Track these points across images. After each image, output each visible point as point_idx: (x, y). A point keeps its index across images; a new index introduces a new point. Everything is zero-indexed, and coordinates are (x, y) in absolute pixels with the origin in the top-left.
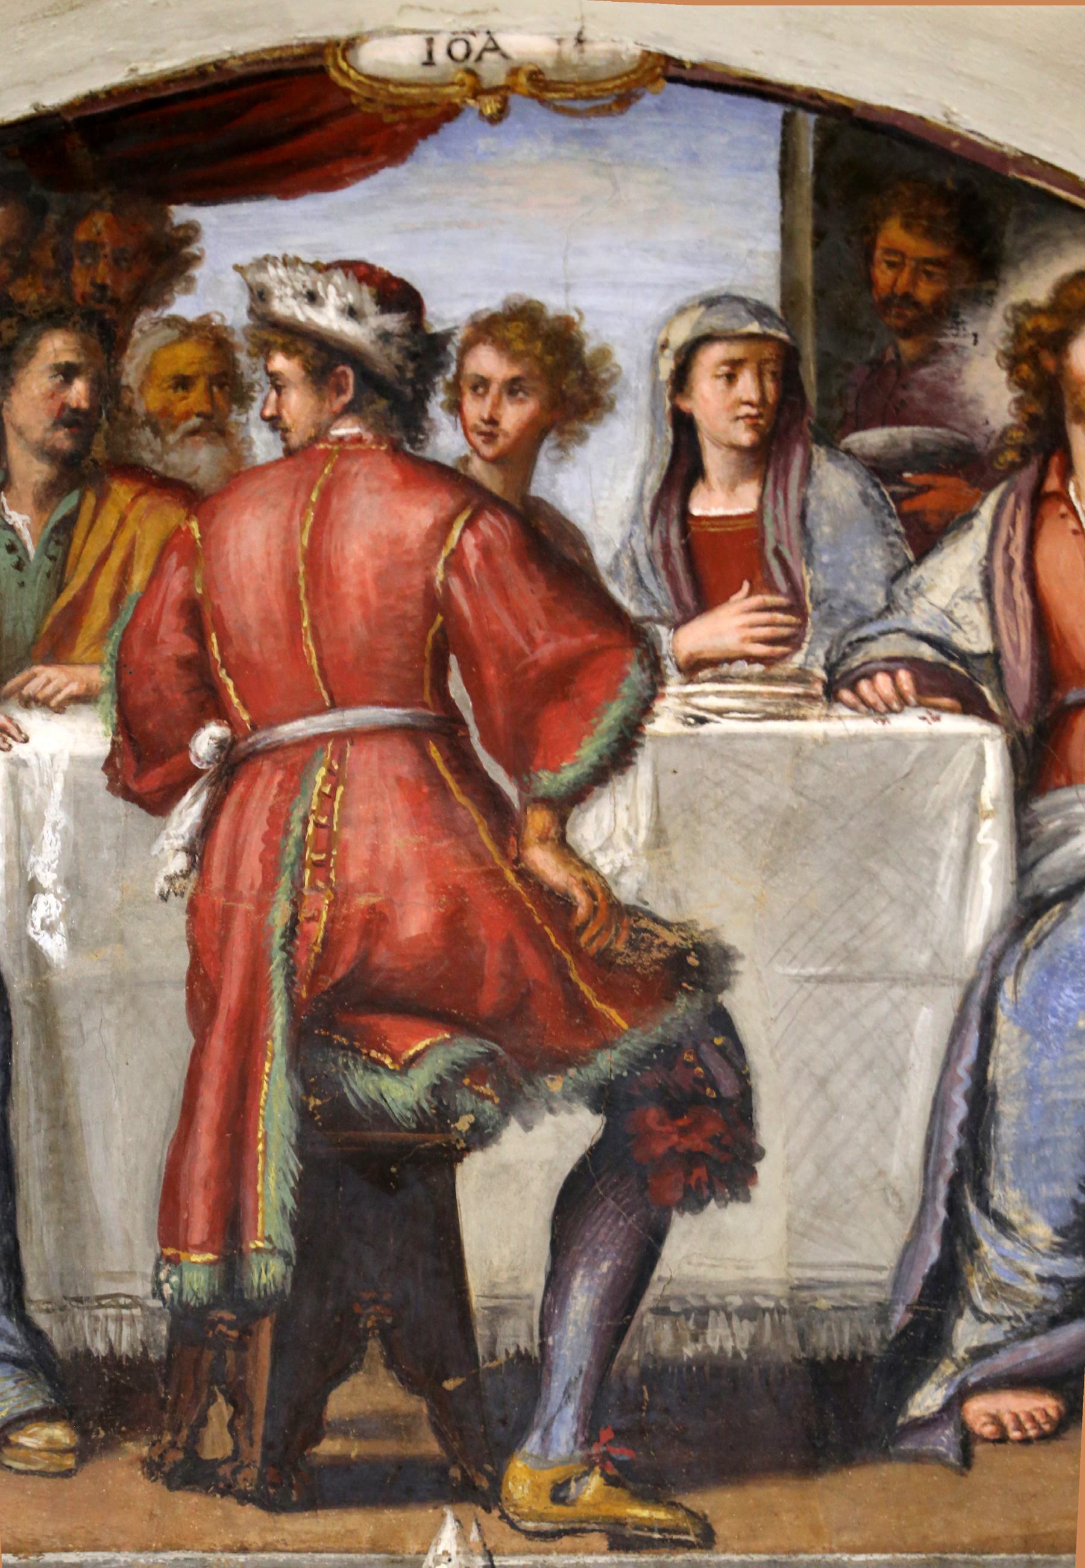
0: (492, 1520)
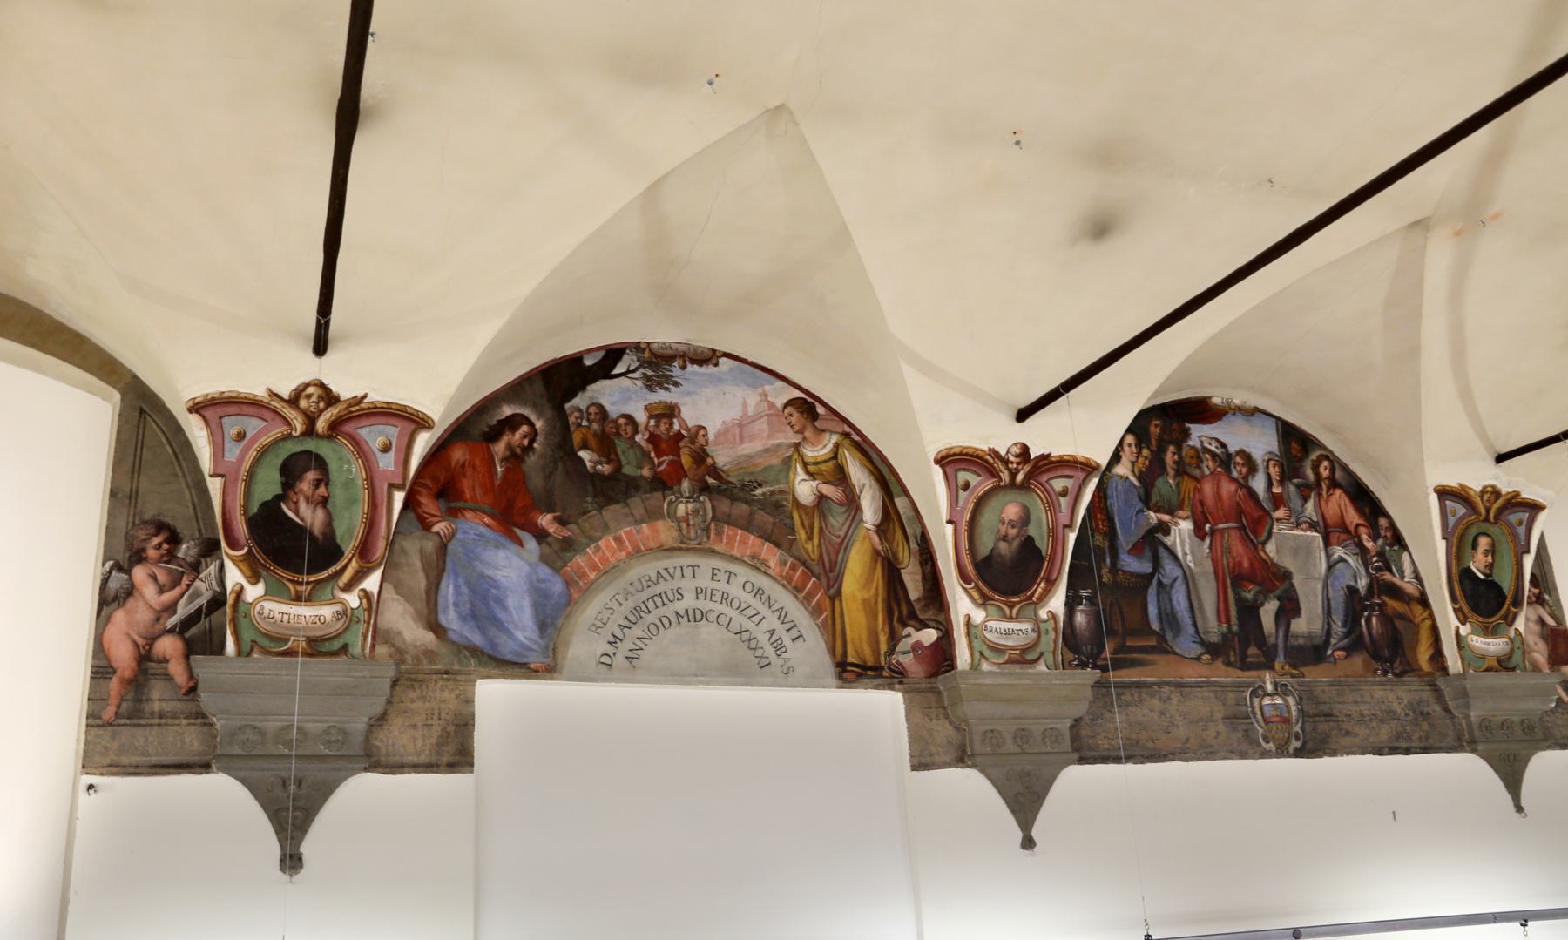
0: (1274, 673)
